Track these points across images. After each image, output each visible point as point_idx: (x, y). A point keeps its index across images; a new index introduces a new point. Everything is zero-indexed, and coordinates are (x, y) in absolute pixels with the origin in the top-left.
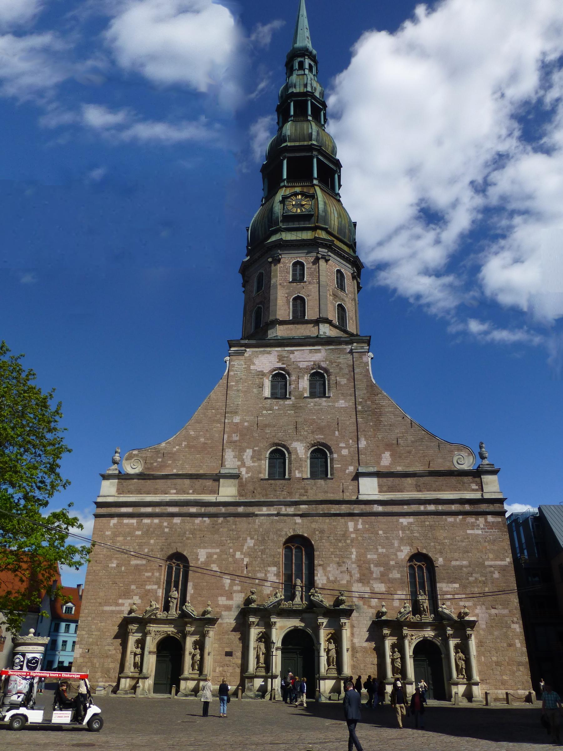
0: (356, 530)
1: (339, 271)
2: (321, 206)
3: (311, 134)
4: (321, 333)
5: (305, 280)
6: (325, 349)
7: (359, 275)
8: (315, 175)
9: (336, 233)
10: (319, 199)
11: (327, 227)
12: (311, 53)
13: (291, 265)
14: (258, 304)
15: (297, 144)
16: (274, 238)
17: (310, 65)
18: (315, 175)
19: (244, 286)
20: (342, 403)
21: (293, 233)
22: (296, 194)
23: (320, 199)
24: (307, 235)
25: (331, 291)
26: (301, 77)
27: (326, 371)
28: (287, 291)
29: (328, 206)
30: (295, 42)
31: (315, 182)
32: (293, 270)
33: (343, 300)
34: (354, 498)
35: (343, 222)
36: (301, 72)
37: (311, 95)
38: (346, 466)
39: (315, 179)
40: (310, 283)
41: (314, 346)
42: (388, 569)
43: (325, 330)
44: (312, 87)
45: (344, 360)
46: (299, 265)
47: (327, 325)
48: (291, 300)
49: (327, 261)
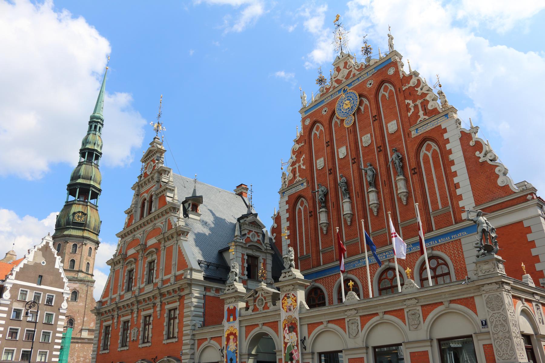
0: (78, 347)
1: (90, 248)
2: (88, 219)
16: (66, 233)
17: (100, 128)
20: (81, 304)
22: (79, 212)
23: (89, 216)
27: (78, 291)
34: (79, 337)
36: (94, 132)
38: (79, 326)
42: (86, 358)
43: (81, 275)
45: (84, 288)
46: (75, 246)
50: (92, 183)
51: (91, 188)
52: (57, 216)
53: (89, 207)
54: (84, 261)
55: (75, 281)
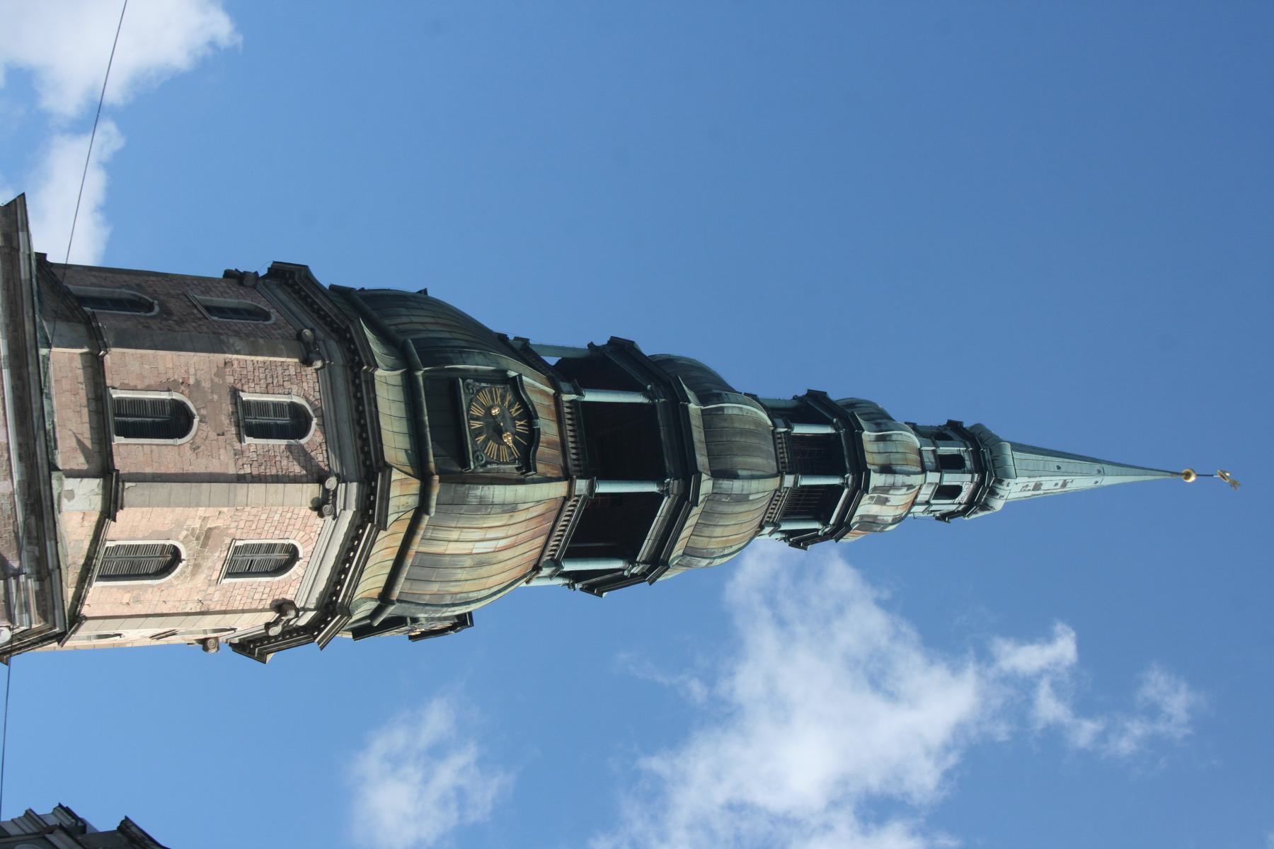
1: (292, 555)
2: (499, 493)
3: (733, 476)
4: (70, 484)
5: (249, 440)
6: (12, 494)
7: (294, 637)
8: (603, 488)
9: (416, 547)
10: (521, 489)
11: (433, 510)
12: (993, 493)
13: (296, 400)
14: (161, 304)
15: (698, 435)
17: (954, 491)
18: (603, 488)
19: (228, 274)
21: (403, 406)
22: (529, 414)
24: (394, 441)
25: (220, 523)
26: (915, 457)
28: (206, 385)
29: (504, 519)
30: (1017, 447)
31: (581, 486)
32: (277, 405)
33: (197, 567)
35: (461, 574)
36: (929, 459)
37: (860, 487)
39: (591, 487)
40: (239, 454)
41: (20, 458)
44: (886, 489)
47: (97, 503)
48: (176, 396)
49: (318, 507)
50: (706, 486)
51: (674, 485)
52: (425, 291)
53: (560, 489)
54: (196, 517)
55: (27, 455)
